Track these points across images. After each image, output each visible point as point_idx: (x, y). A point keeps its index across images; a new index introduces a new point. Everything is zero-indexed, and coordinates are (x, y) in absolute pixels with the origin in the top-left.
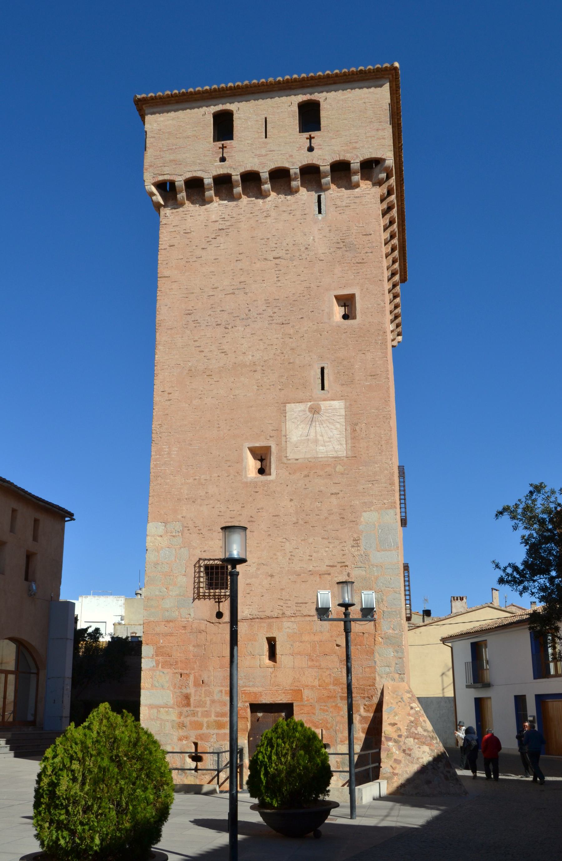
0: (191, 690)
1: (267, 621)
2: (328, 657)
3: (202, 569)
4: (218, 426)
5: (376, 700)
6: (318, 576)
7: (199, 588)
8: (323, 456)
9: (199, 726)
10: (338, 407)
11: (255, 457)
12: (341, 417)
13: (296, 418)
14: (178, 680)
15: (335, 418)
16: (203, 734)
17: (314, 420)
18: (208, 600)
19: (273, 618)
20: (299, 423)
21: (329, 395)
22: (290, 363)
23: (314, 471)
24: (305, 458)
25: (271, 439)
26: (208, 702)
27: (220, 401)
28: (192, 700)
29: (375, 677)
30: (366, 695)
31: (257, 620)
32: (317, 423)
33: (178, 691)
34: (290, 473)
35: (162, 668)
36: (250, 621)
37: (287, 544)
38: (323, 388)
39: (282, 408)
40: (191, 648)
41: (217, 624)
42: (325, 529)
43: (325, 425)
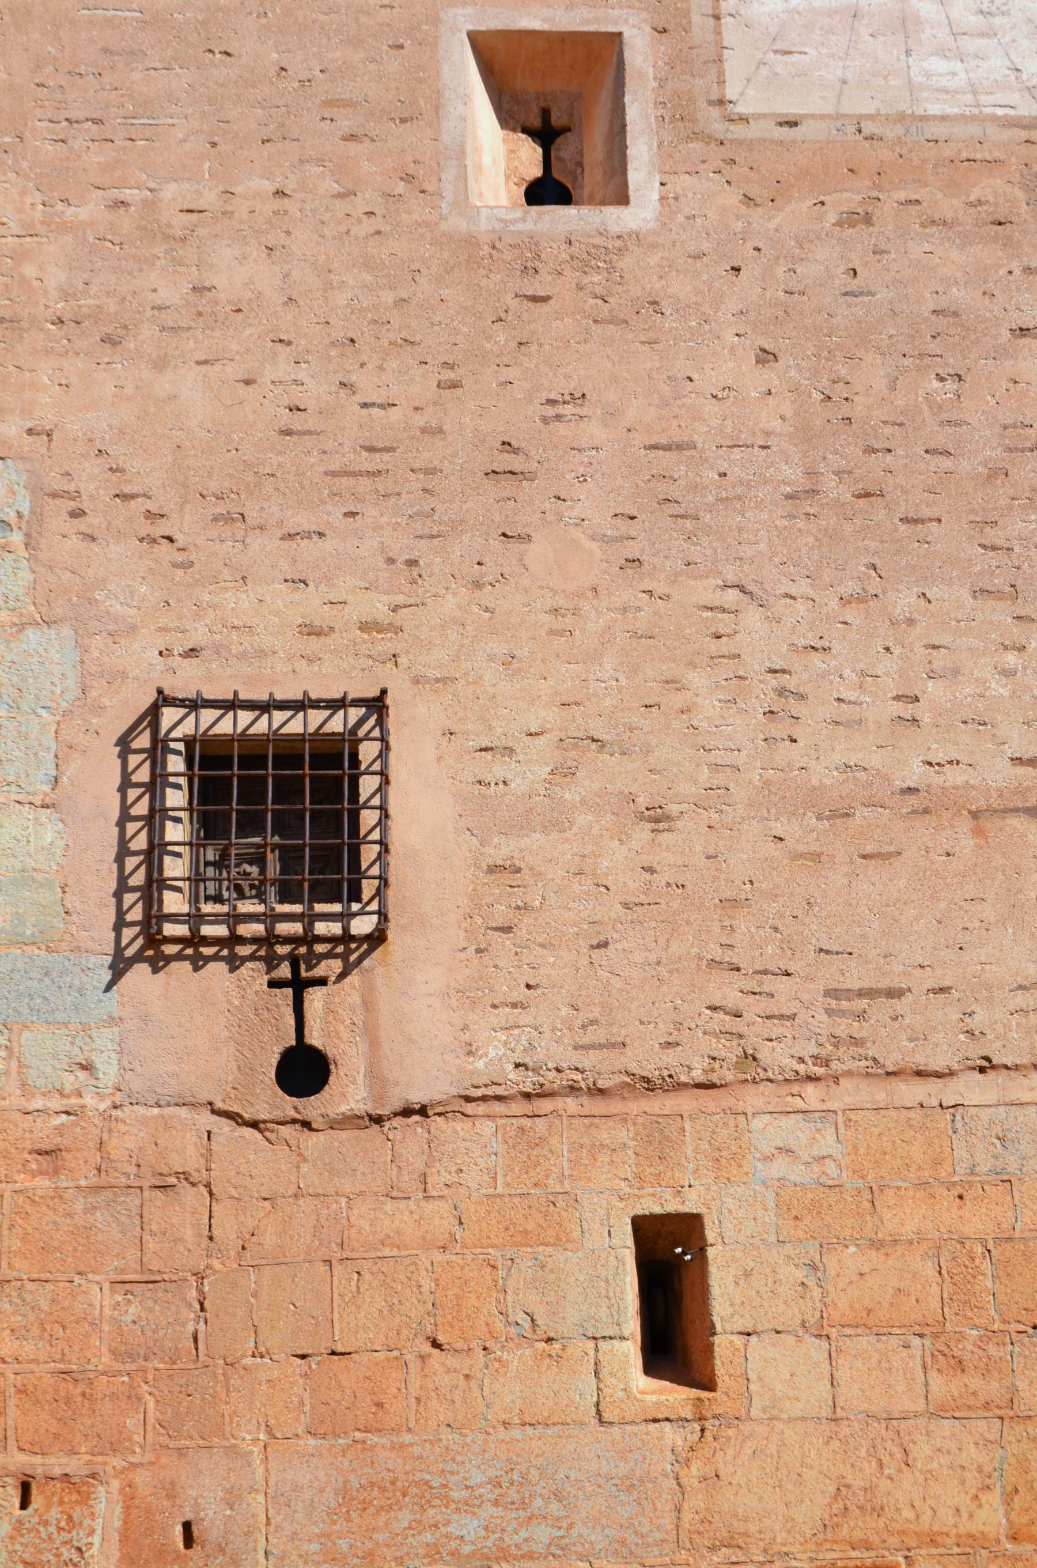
1: (635, 1107)
3: (176, 764)
6: (964, 825)
7: (155, 885)
18: (222, 967)
19: (682, 1086)
31: (571, 1104)
34: (748, 199)
36: (518, 1107)
37: (753, 617)
40: (100, 1298)
41: (286, 1131)
42: (992, 535)
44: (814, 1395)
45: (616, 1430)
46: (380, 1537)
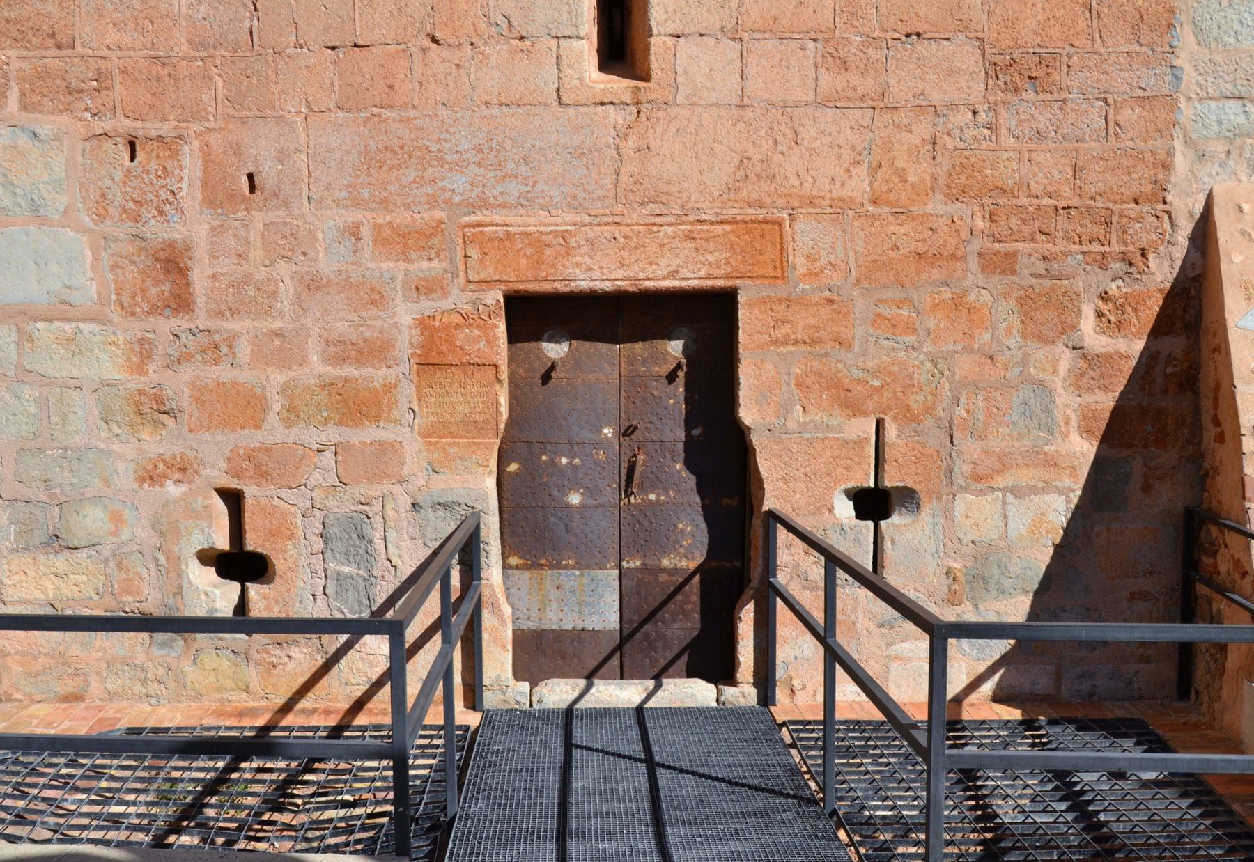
0: (192, 225)
2: (923, 48)
5: (1162, 272)
9: (245, 407)
14: (119, 175)
16: (268, 450)
26: (287, 290)
28: (199, 277)
29: (1170, 153)
30: (1116, 248)
33: (120, 230)
35: (25, 108)
44: (727, 87)
45: (571, 111)
46: (392, 188)
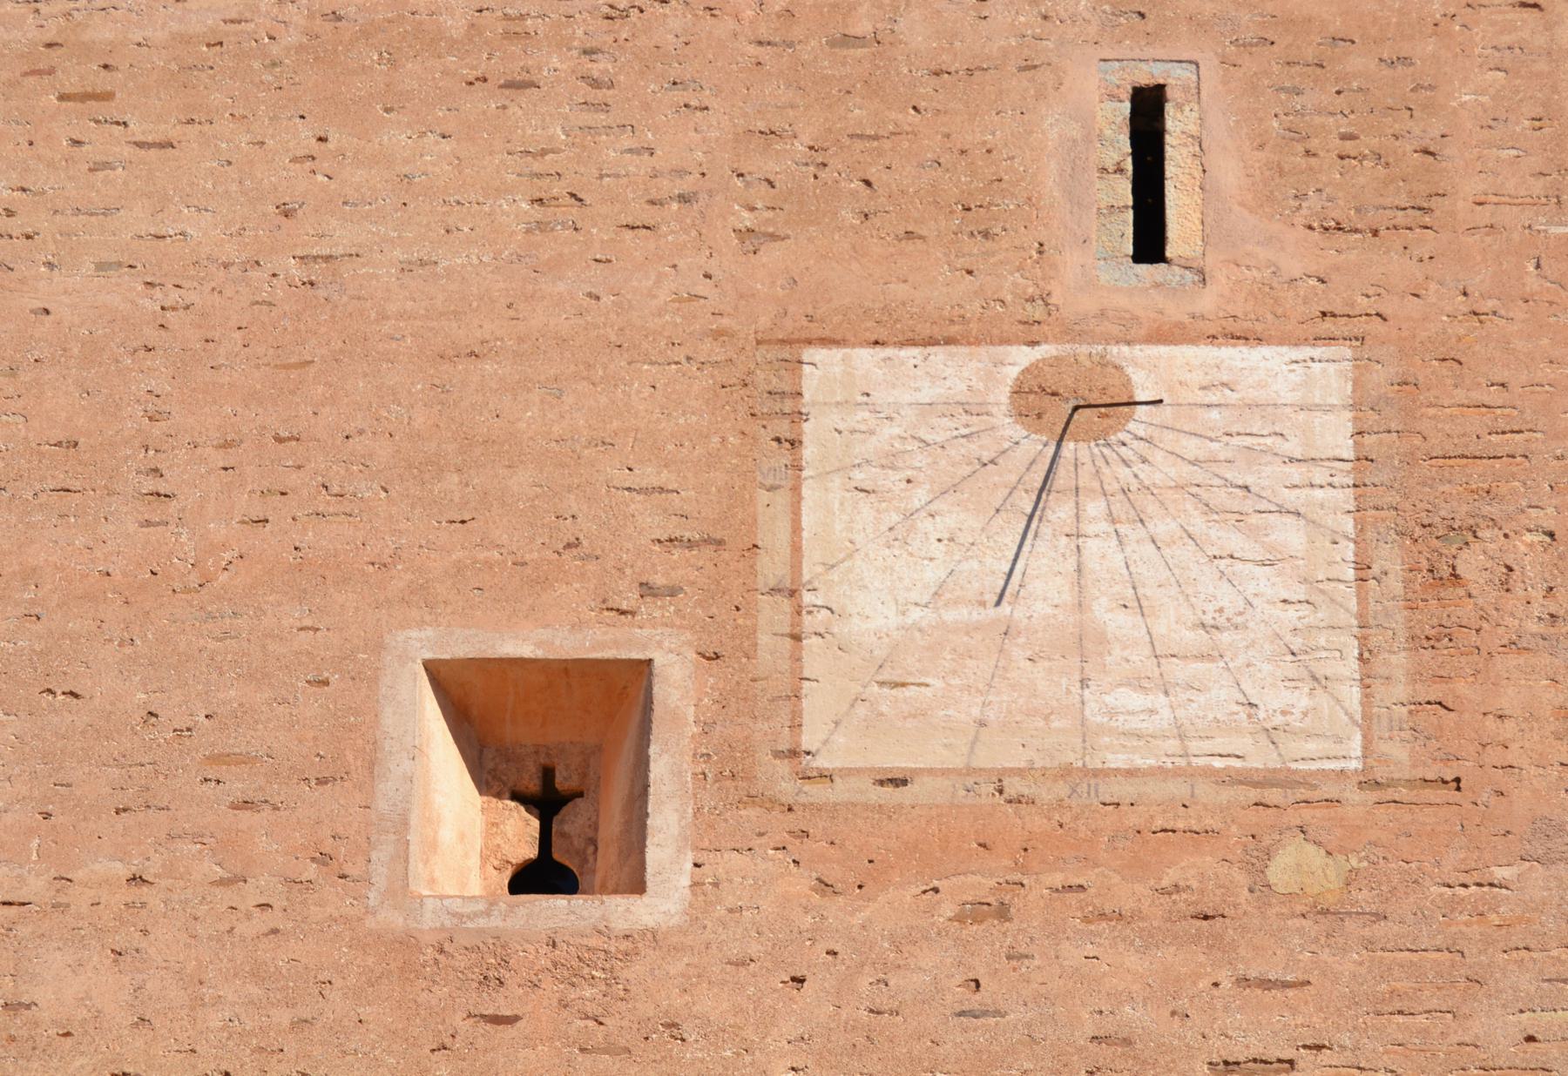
4: (150, 484)
8: (1139, 762)
10: (1289, 397)
11: (489, 766)
12: (1320, 475)
13: (890, 461)
15: (1268, 477)
17: (1062, 478)
20: (920, 495)
21: (1206, 302)
22: (848, 40)
23: (1058, 879)
24: (971, 771)
25: (647, 609)
27: (174, 296)
32: (1094, 507)
38: (1150, 243)
39: (764, 379)
43: (1163, 527)
